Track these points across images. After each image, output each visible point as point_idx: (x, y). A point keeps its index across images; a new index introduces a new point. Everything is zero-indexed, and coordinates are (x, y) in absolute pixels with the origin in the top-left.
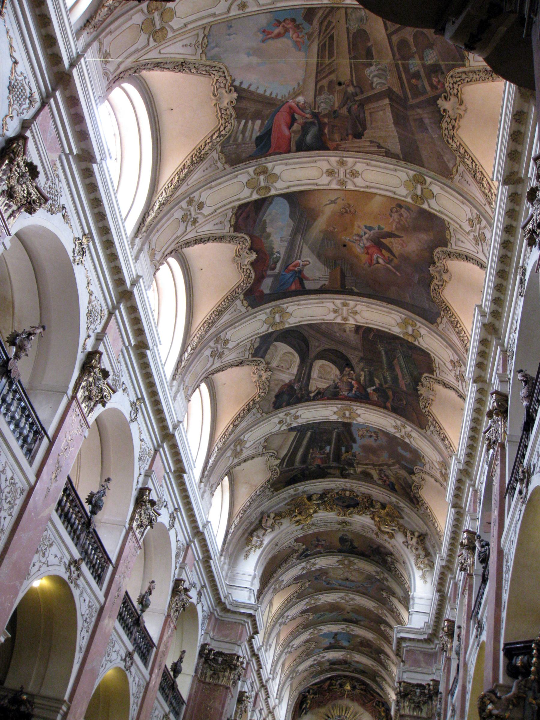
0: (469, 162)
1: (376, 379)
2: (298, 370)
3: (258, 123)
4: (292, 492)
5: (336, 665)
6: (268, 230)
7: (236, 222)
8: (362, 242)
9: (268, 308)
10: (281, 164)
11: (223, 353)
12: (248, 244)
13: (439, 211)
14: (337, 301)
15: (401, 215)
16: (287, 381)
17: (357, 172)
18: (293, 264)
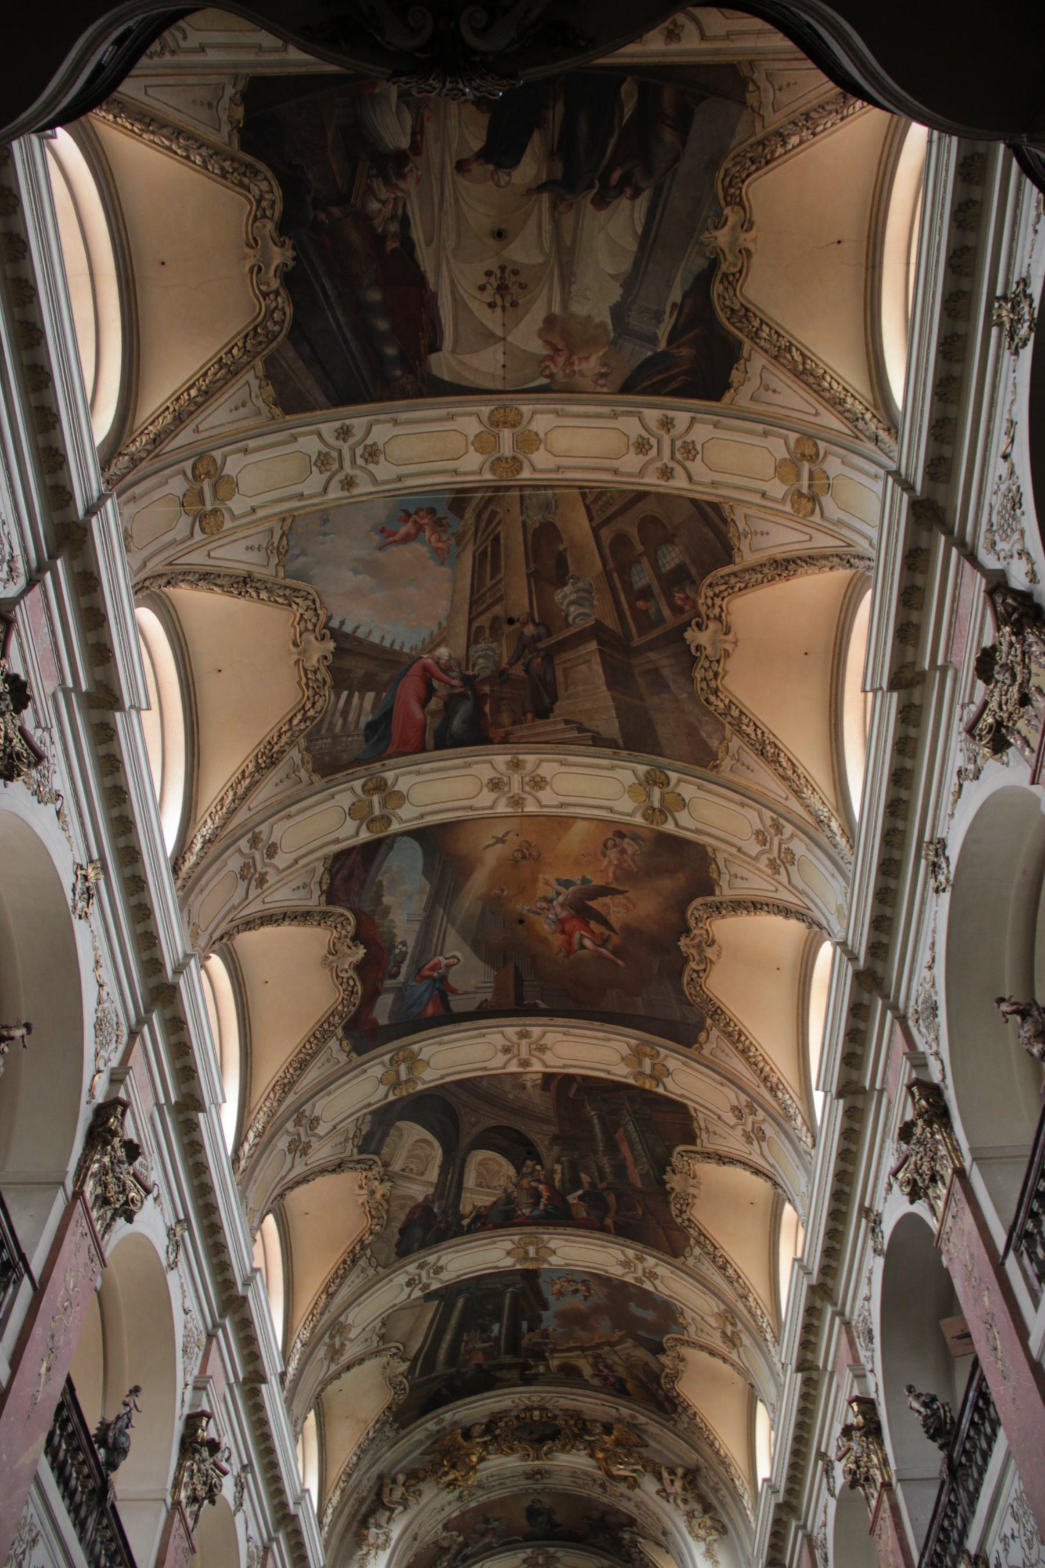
0: (750, 730)
1: (583, 1176)
2: (440, 1175)
3: (370, 696)
4: (431, 1426)
6: (386, 900)
7: (331, 885)
9: (385, 1053)
10: (410, 773)
11: (308, 1145)
12: (351, 929)
13: (697, 831)
14: (509, 1030)
15: (623, 851)
16: (421, 1198)
17: (543, 779)
18: (427, 966)
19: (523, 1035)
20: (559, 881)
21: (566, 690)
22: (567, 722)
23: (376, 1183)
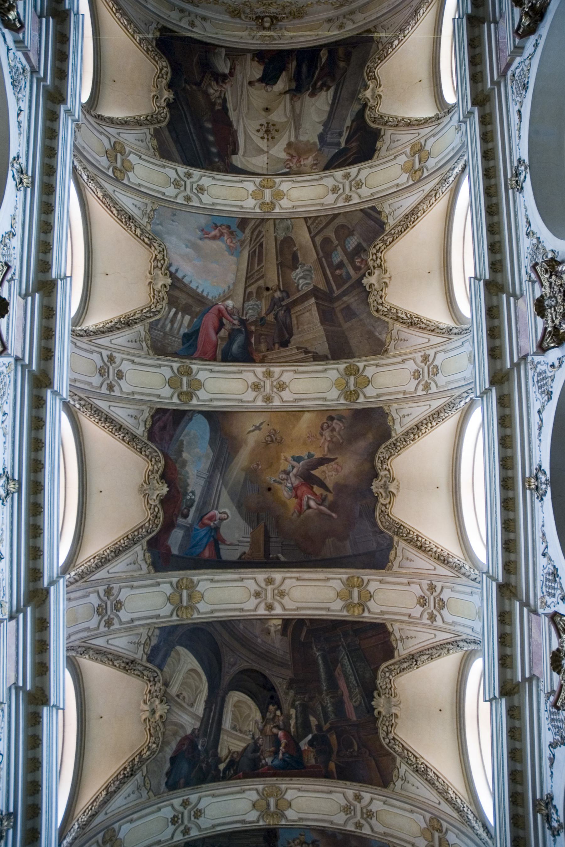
8: (289, 481)
18: (207, 516)
19: (269, 581)
20: (293, 457)
21: (298, 328)
22: (298, 348)
23: (157, 702)
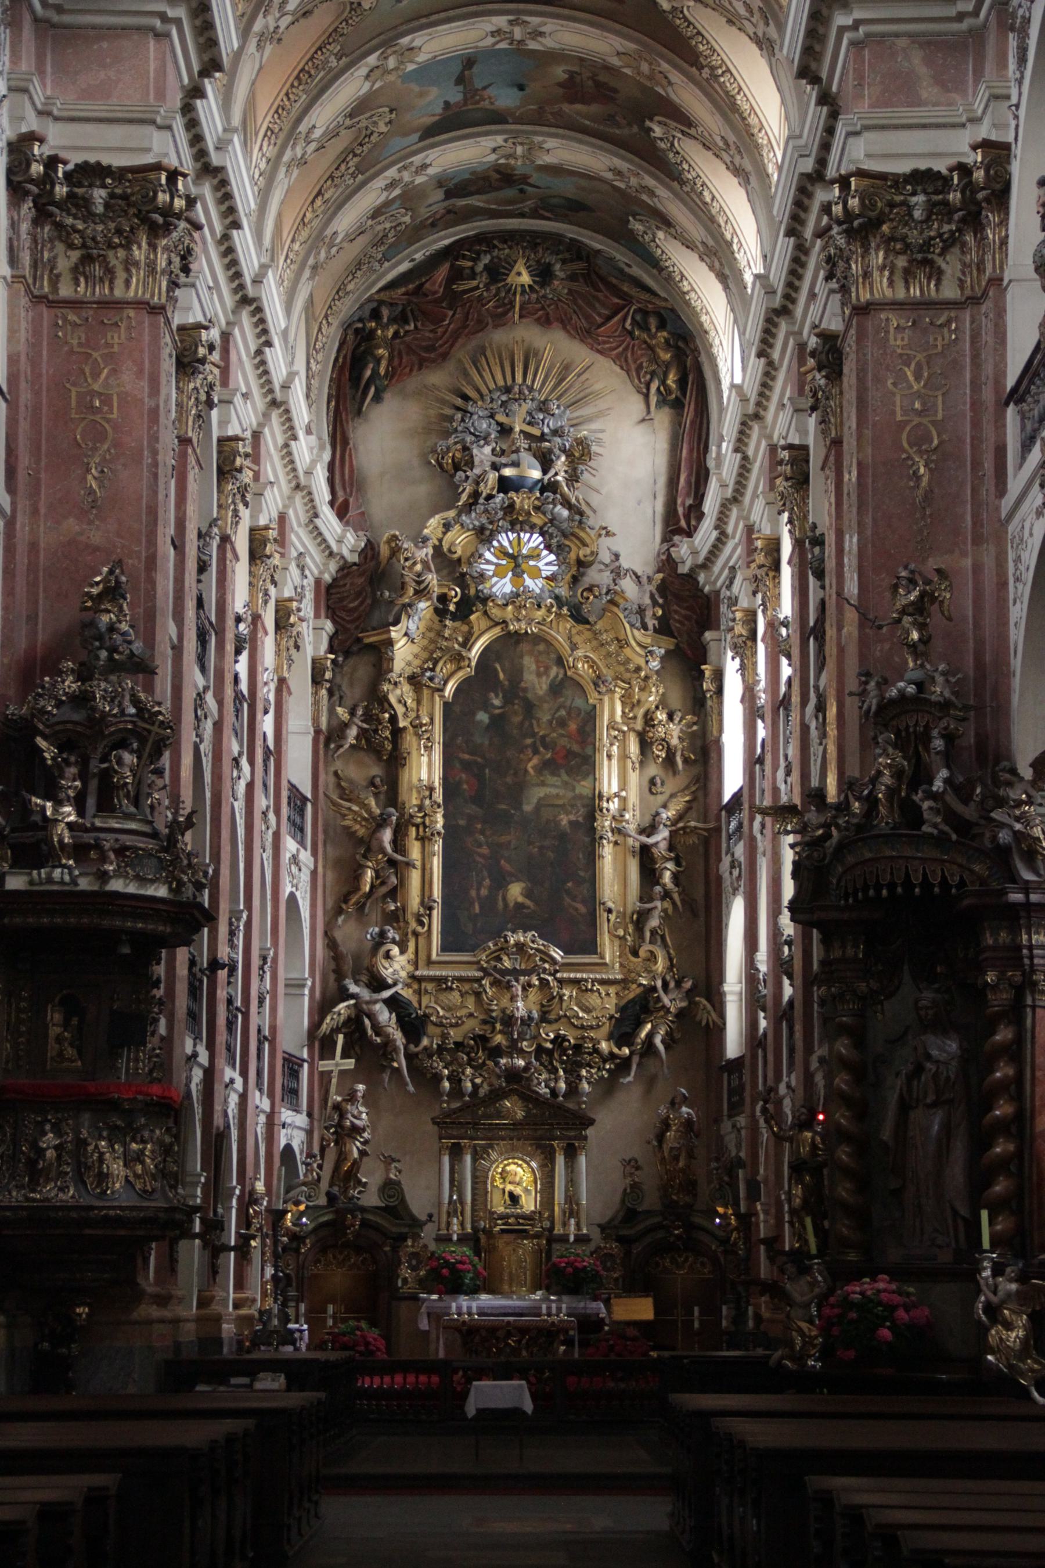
5: (471, 194)
